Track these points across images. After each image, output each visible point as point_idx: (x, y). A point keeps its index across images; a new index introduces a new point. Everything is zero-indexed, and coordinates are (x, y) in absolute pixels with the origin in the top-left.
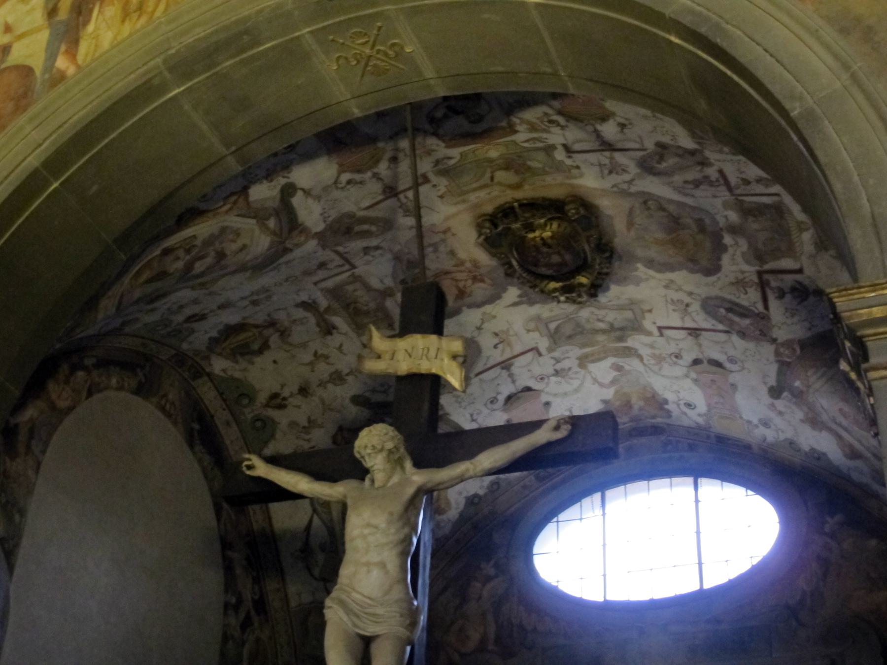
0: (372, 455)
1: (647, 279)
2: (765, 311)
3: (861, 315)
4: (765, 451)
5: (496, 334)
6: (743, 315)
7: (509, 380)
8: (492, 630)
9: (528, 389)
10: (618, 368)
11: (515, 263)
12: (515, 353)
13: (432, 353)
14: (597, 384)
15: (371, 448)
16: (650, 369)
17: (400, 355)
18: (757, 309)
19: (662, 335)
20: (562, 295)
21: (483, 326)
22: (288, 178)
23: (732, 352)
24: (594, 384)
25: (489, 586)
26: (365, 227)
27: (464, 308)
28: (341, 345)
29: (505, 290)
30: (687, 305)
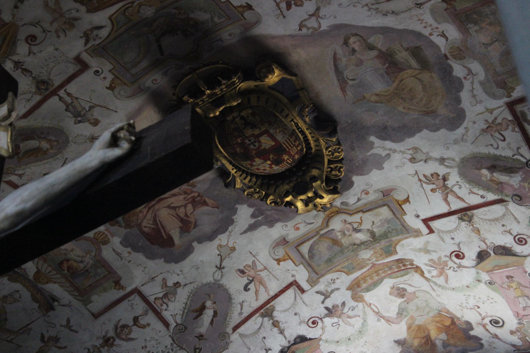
1: (388, 156)
5: (242, 272)
6: (510, 170)
7: (276, 330)
9: (302, 339)
10: (401, 293)
11: (230, 167)
12: (272, 293)
14: (382, 320)
16: (436, 284)
18: (526, 158)
19: (431, 231)
20: (295, 197)
21: (223, 264)
23: (516, 229)
24: (378, 320)
26: (33, 144)
28: (68, 321)
29: (234, 211)
30: (445, 179)
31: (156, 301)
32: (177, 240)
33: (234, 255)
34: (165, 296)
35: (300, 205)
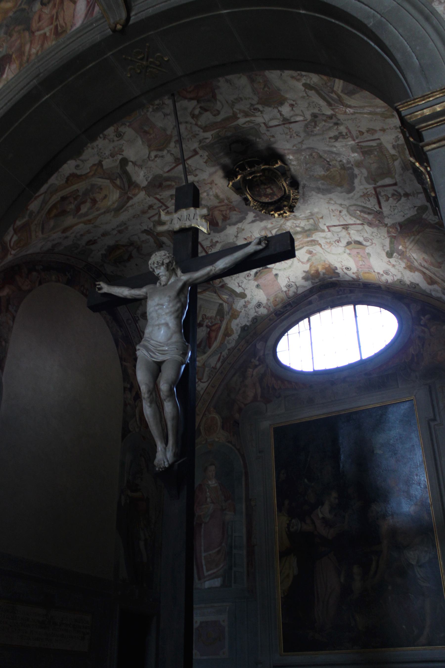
0: (158, 267)
2: (380, 210)
3: (417, 115)
4: (388, 288)
8: (259, 390)
10: (310, 252)
11: (249, 197)
13: (192, 216)
14: (300, 262)
15: (157, 263)
16: (326, 251)
17: (175, 221)
18: (376, 209)
19: (329, 231)
20: (275, 212)
21: (239, 235)
22: (123, 155)
23: (366, 235)
24: (299, 262)
25: (256, 370)
26: (169, 183)
27: (228, 226)
29: (247, 214)
30: (340, 212)
31: (207, 248)
32: (220, 224)
33: (243, 232)
34: (211, 246)
35: (276, 215)
